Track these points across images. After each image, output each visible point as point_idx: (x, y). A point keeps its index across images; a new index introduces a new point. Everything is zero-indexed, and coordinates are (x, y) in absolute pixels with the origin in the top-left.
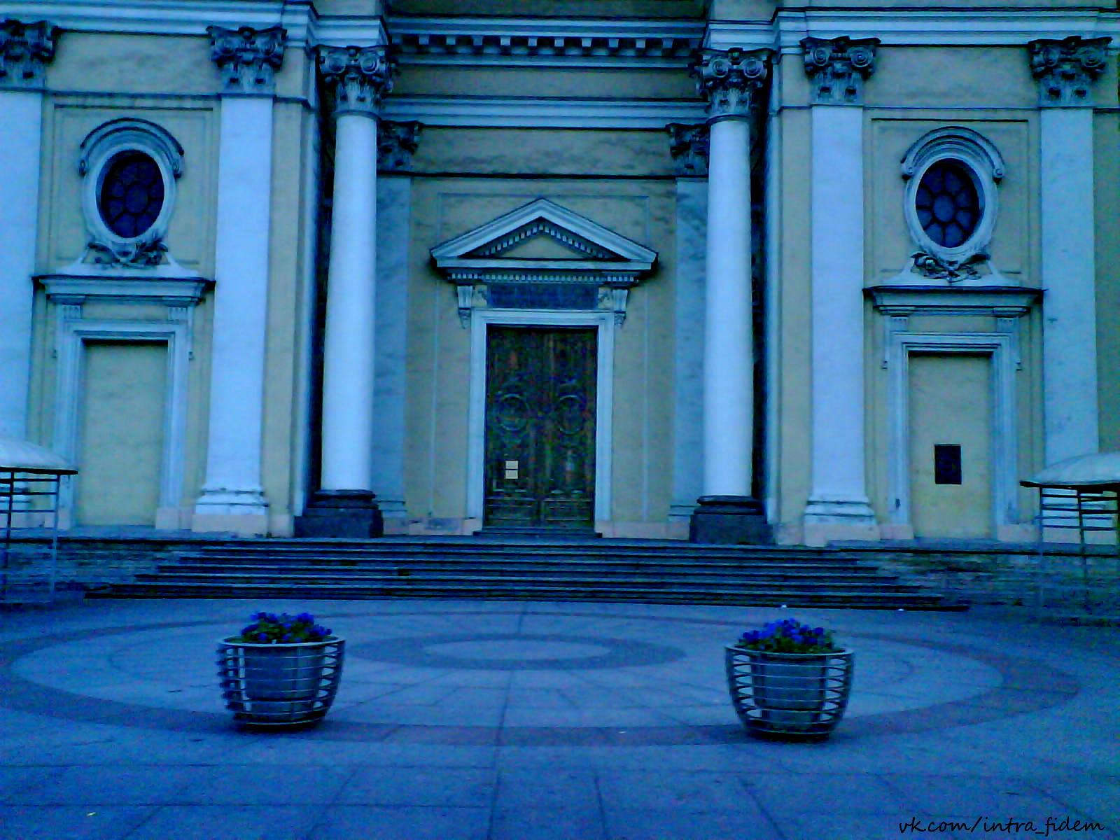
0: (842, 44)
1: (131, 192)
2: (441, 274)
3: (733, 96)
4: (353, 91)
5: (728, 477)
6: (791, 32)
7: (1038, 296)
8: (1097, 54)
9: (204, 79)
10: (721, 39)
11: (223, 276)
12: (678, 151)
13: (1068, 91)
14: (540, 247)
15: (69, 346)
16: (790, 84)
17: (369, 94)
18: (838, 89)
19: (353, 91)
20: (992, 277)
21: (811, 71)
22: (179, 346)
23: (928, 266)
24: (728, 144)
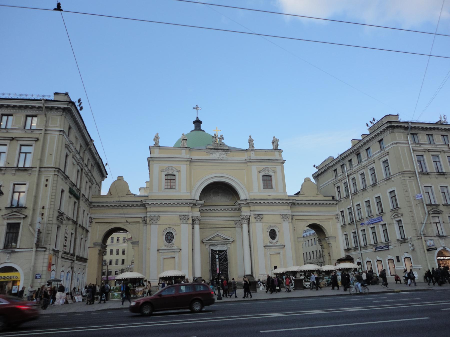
0: (259, 215)
1: (169, 237)
2: (204, 243)
3: (245, 221)
4: (197, 222)
5: (248, 272)
6: (252, 213)
7: (285, 246)
8: (288, 216)
9: (179, 222)
10: (243, 213)
11: (182, 249)
12: (236, 224)
13: (285, 220)
14: (217, 238)
15: (162, 259)
16: (252, 220)
17: (199, 222)
18: (259, 220)
19: (197, 222)
20: (279, 244)
21: (256, 218)
22: (177, 259)
23: (271, 243)
24: (245, 226)
